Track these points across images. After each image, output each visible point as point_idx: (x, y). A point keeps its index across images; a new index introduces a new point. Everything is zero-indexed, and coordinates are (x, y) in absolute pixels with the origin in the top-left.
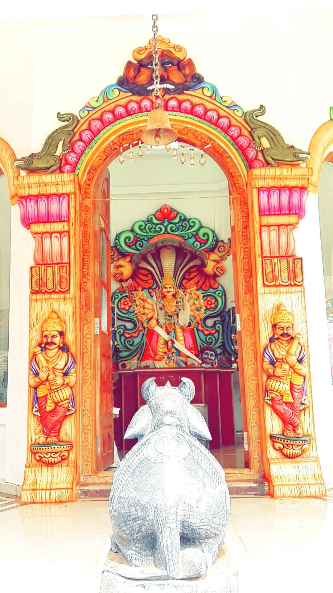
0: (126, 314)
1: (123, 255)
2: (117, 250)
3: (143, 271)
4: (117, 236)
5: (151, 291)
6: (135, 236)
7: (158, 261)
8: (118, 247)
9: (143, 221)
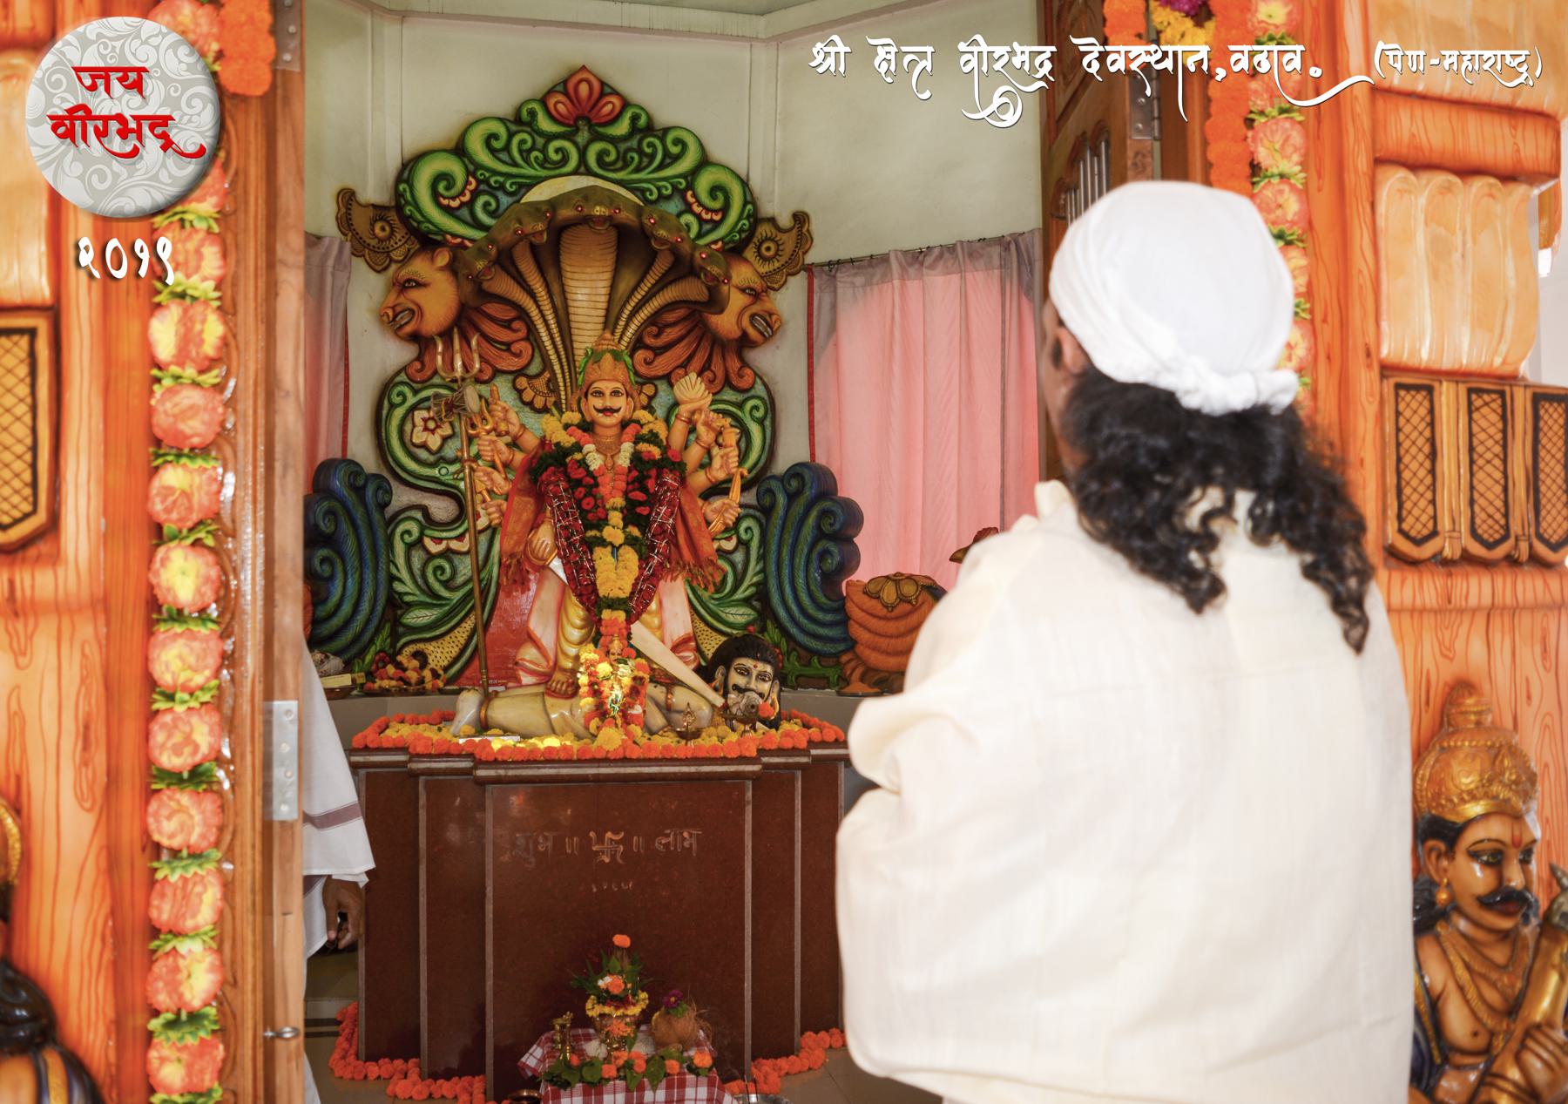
0: (432, 465)
1: (428, 241)
2: (405, 220)
3: (493, 309)
4: (404, 166)
5: (522, 382)
6: (468, 173)
7: (551, 275)
8: (408, 210)
9: (502, 120)
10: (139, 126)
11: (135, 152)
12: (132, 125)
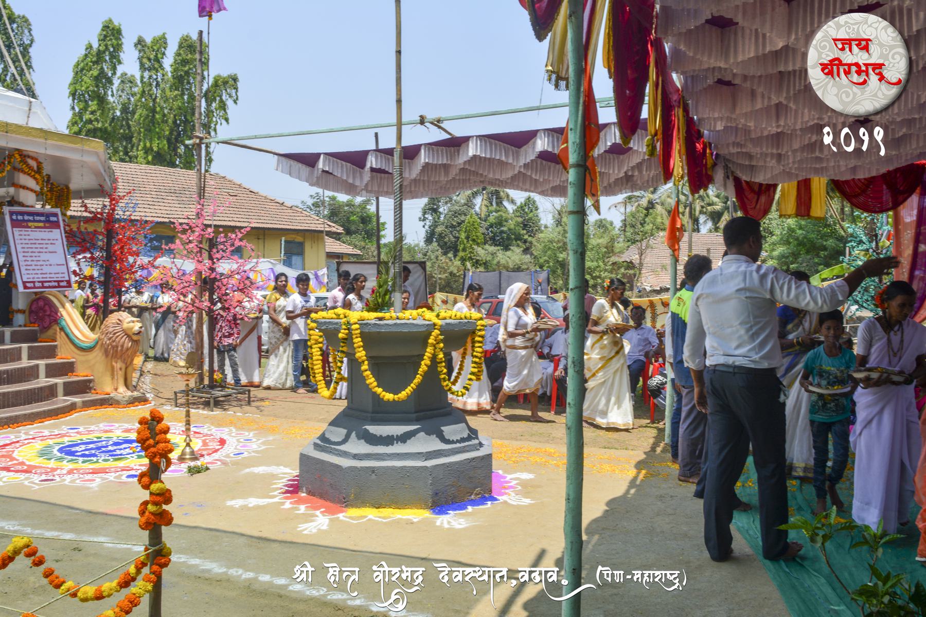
10: (867, 69)
11: (865, 82)
12: (864, 68)
